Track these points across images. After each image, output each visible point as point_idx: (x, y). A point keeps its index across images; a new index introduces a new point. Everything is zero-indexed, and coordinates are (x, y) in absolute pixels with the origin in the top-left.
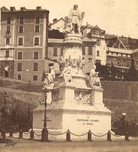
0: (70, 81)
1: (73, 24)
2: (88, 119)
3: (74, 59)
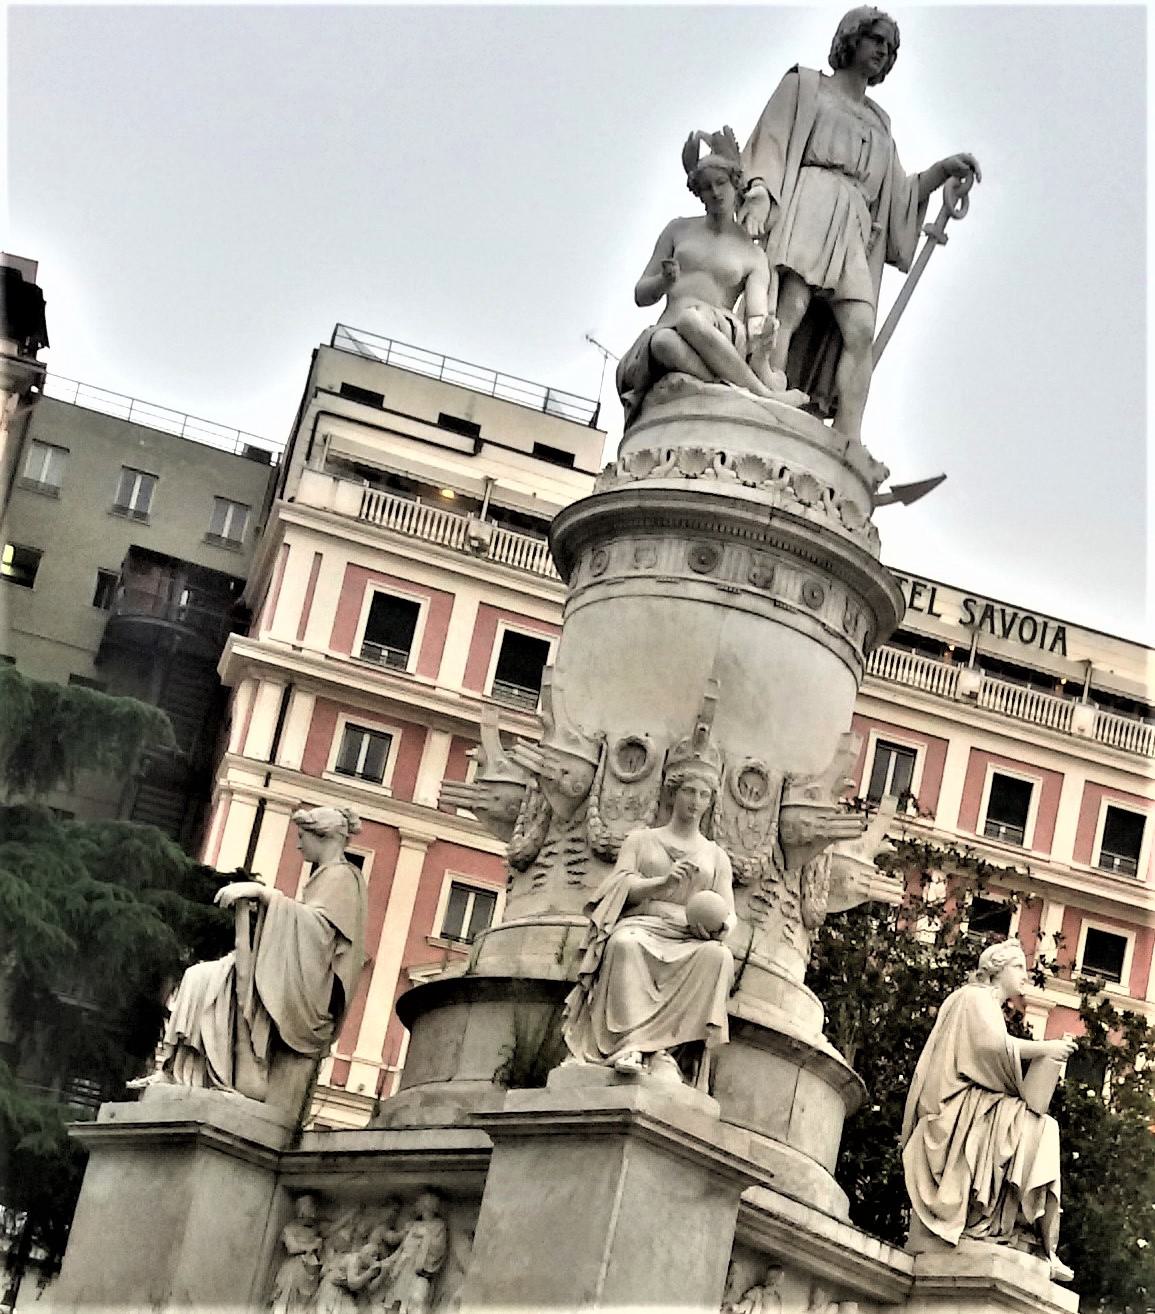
0: (689, 1057)
3: (752, 770)
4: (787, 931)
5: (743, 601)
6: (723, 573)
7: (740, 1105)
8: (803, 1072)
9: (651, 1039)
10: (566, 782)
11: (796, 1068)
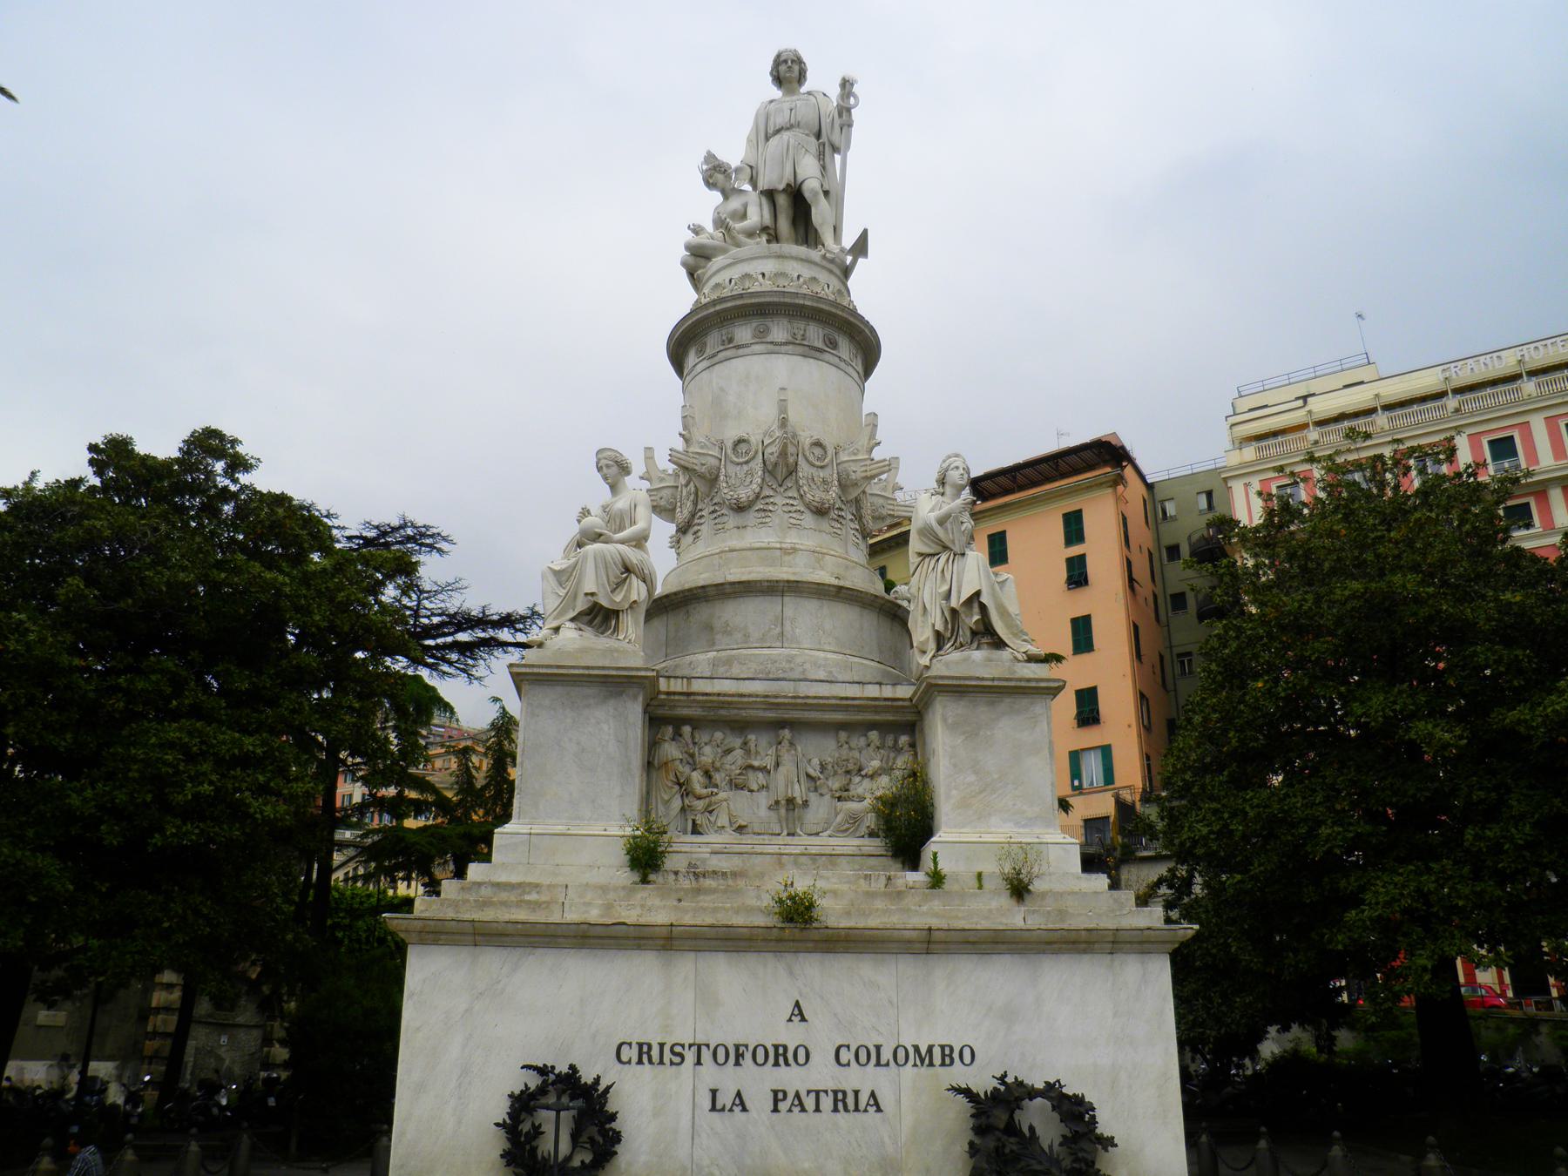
1: (770, 194)
2: (791, 1036)
3: (740, 441)
4: (792, 521)
5: (721, 356)
6: (709, 351)
7: (738, 636)
8: (786, 599)
9: (555, 619)
10: (663, 503)
11: (780, 598)
